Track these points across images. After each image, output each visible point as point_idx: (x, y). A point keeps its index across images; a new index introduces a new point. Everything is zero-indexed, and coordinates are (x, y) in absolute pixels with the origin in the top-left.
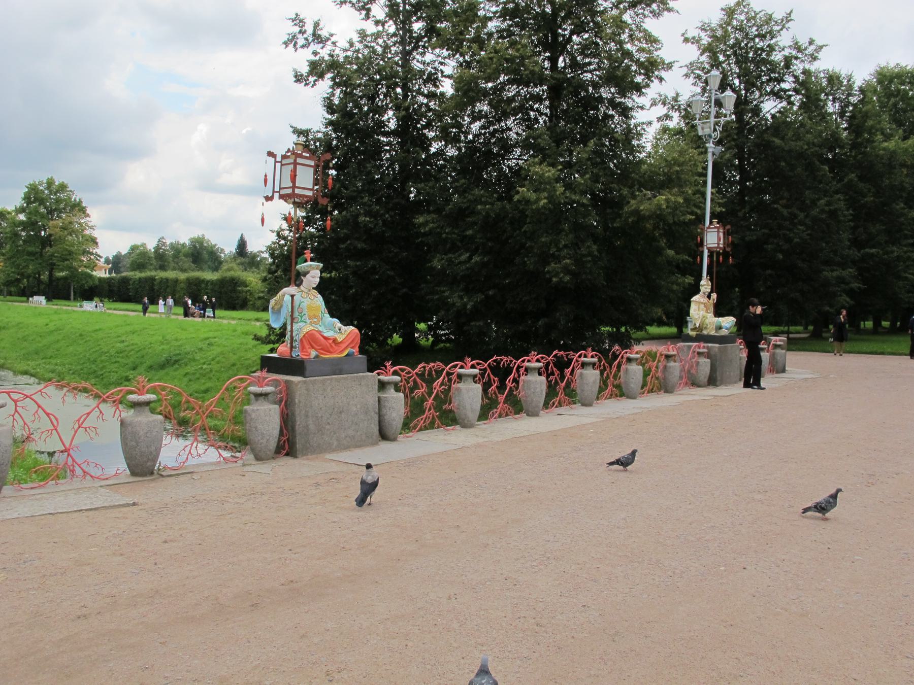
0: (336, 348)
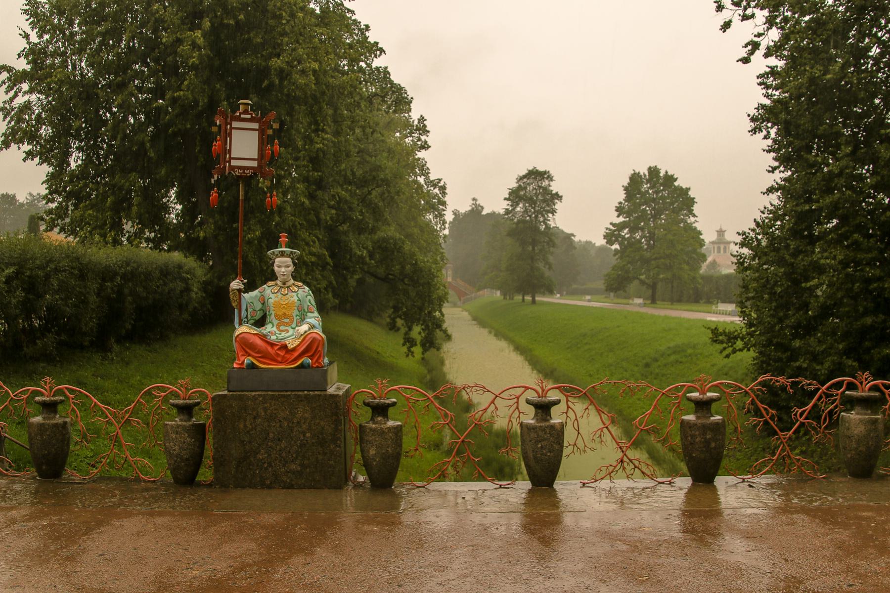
0: (288, 356)
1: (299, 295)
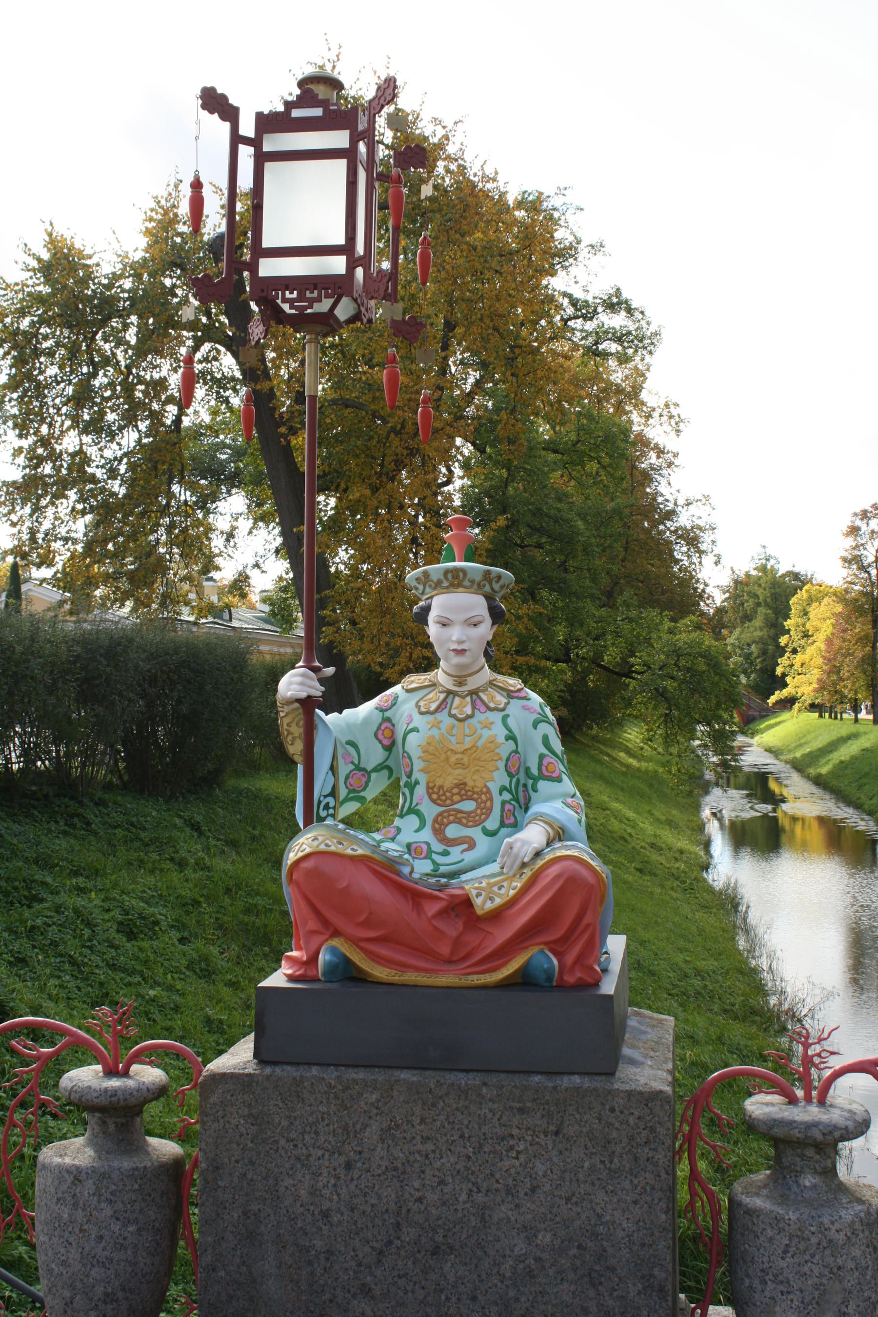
1: (510, 721)
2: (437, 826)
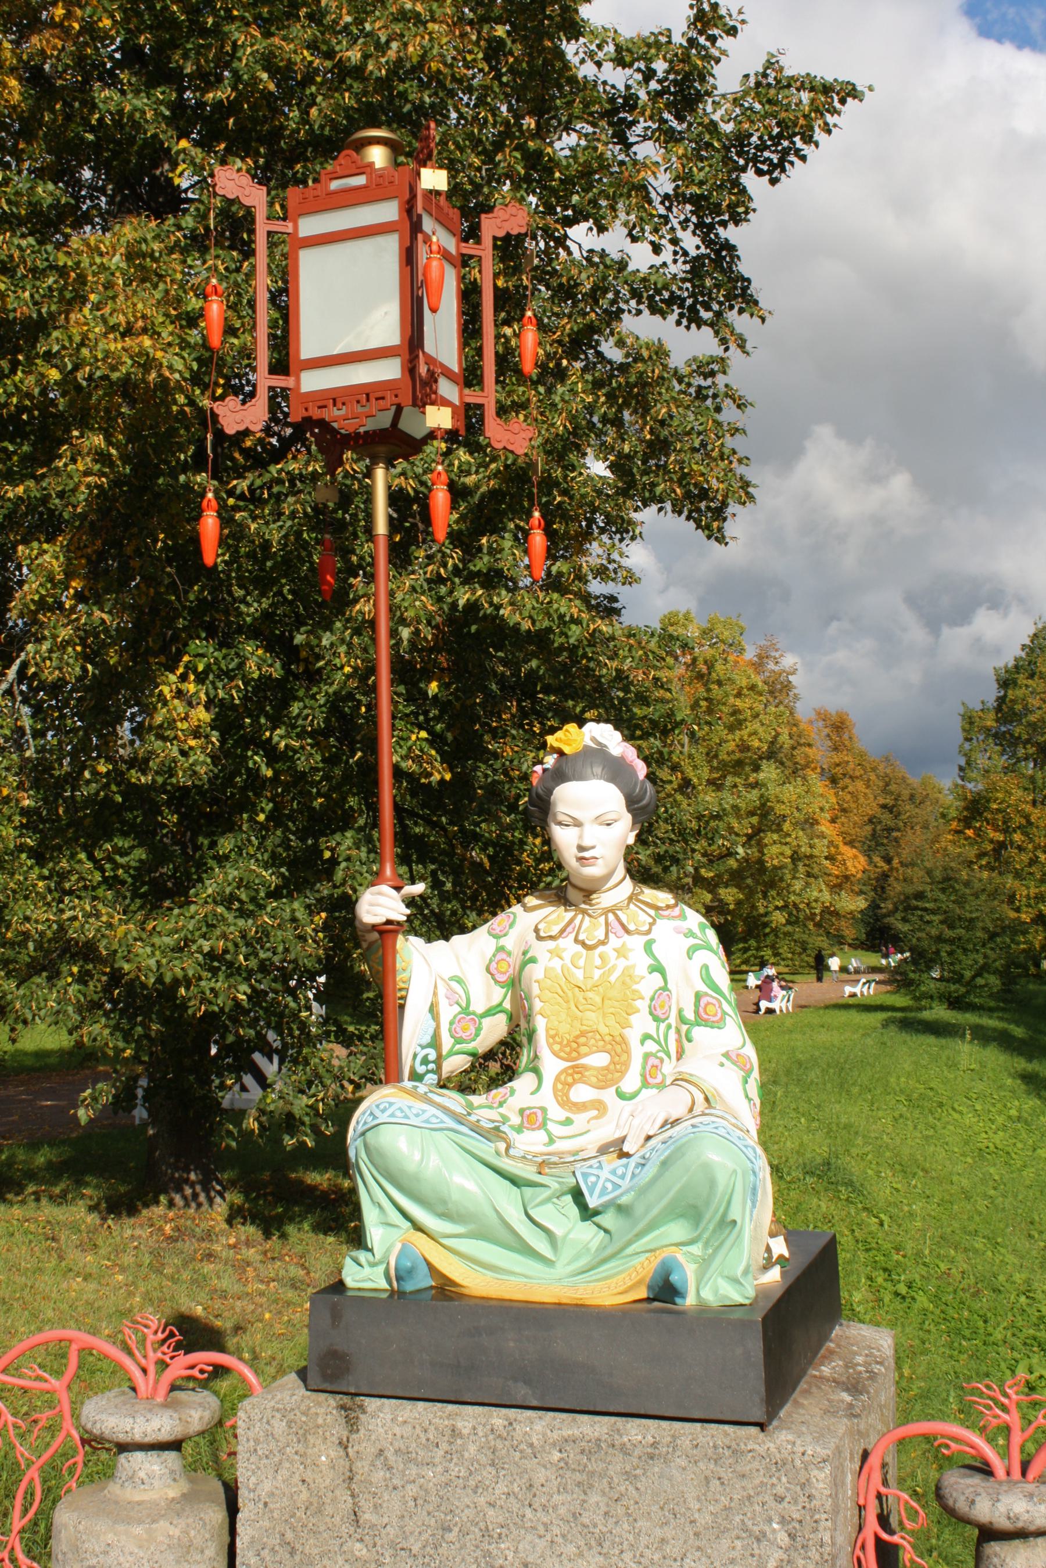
2: (560, 1086)
